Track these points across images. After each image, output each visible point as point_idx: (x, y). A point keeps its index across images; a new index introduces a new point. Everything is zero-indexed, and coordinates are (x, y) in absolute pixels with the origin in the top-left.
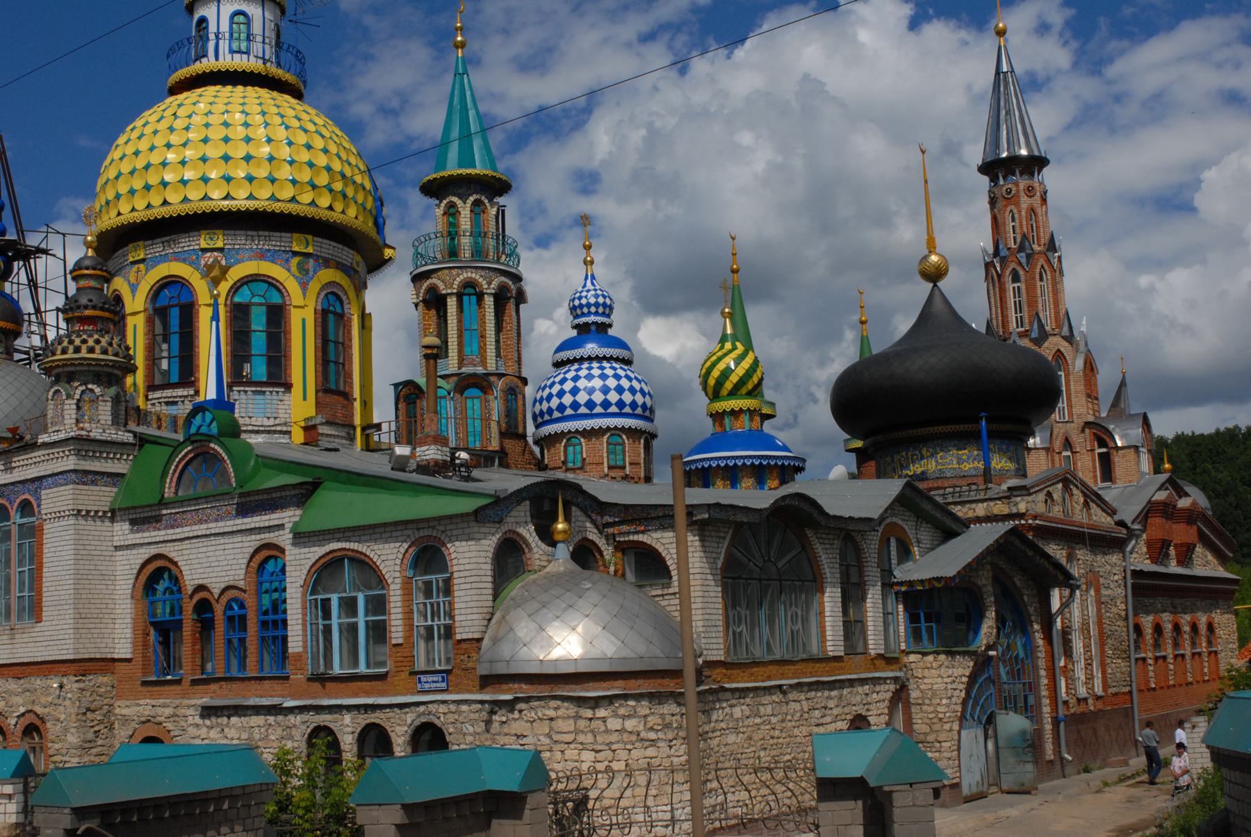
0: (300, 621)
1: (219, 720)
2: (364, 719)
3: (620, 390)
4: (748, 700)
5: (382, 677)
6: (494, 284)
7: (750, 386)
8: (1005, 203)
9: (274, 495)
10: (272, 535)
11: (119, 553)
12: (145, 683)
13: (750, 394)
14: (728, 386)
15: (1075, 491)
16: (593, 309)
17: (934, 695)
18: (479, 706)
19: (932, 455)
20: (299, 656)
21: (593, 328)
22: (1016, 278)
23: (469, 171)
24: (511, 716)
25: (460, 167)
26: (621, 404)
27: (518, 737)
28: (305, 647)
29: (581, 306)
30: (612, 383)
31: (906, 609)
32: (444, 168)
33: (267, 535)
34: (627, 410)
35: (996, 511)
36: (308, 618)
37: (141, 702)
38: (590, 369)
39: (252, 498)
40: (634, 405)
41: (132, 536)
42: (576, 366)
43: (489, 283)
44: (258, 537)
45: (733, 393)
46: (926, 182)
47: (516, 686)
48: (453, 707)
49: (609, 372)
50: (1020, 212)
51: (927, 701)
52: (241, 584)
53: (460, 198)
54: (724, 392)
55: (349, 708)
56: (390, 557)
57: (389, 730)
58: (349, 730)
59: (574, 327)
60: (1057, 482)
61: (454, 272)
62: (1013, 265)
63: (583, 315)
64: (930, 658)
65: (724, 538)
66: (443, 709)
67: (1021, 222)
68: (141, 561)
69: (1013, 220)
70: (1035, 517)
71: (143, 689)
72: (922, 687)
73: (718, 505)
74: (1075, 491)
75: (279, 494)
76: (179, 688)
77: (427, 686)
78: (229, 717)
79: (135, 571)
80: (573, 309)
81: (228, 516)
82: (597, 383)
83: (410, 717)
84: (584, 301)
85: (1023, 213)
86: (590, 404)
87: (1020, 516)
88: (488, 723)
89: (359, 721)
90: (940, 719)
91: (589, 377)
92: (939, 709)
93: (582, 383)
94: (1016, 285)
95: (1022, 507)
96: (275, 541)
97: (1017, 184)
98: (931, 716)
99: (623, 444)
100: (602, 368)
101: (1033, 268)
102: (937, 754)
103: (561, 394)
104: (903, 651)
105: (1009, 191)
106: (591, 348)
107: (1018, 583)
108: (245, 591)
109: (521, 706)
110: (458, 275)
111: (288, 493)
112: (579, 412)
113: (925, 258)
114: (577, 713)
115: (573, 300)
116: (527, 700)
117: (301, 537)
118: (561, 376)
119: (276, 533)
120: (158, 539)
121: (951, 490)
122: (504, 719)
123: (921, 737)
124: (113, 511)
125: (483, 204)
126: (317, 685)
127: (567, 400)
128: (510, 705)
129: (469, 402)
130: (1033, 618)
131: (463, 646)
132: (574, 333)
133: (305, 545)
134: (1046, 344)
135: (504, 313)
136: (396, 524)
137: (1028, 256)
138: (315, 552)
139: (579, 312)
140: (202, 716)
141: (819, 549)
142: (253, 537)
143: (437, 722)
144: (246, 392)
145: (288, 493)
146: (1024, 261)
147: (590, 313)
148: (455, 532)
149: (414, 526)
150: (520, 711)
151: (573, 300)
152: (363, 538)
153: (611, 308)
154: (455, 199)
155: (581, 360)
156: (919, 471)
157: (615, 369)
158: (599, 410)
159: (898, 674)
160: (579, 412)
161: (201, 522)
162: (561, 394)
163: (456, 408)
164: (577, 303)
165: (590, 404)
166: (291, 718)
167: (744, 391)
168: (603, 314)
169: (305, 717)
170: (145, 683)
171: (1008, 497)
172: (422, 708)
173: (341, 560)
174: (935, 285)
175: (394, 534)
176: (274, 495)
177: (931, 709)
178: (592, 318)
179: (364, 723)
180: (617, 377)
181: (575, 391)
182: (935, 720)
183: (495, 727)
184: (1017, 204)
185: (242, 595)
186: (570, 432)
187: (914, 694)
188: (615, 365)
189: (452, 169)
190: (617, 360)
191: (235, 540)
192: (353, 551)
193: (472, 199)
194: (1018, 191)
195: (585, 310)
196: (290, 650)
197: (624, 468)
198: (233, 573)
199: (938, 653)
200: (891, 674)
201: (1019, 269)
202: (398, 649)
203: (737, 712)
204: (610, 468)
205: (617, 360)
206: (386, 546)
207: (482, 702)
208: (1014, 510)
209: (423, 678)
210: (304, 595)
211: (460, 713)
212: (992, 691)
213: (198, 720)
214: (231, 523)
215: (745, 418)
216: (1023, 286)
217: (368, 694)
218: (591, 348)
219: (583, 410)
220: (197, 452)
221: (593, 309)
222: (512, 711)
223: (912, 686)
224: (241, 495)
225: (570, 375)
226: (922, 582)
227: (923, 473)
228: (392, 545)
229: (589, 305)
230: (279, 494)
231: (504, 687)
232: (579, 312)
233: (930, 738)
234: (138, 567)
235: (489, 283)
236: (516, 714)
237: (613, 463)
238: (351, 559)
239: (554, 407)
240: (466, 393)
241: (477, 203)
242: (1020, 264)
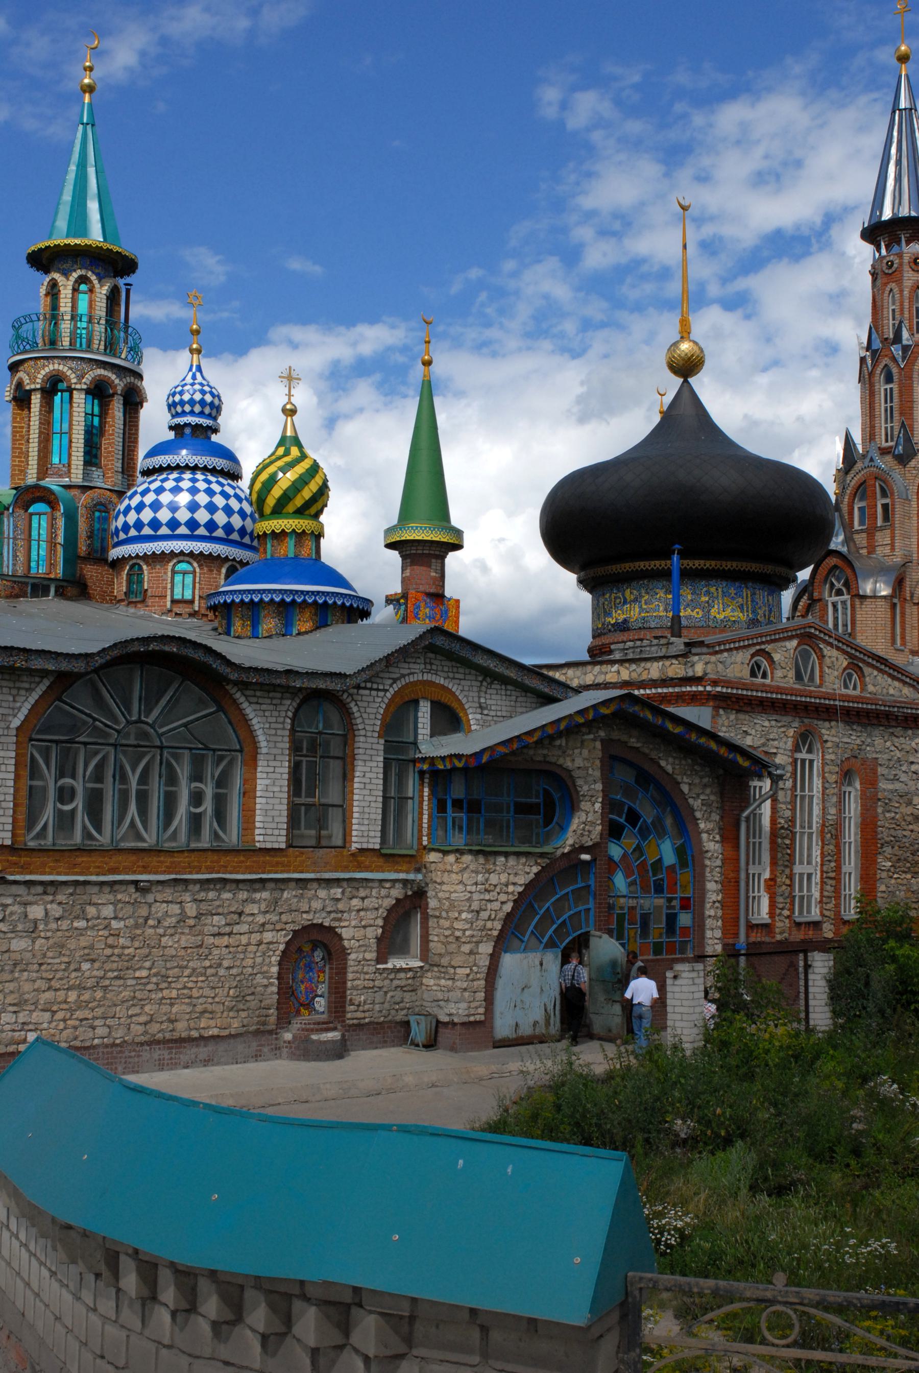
3: (228, 510)
4: (61, 898)
6: (88, 378)
7: (298, 502)
13: (300, 512)
14: (271, 502)
15: (828, 651)
16: (197, 409)
17: (452, 906)
19: (635, 600)
21: (188, 431)
22: (889, 379)
23: (78, 241)
25: (67, 237)
26: (211, 525)
29: (182, 403)
30: (202, 499)
31: (432, 793)
32: (50, 238)
34: (202, 531)
35: (671, 674)
38: (178, 480)
40: (228, 528)
42: (175, 475)
43: (81, 377)
45: (278, 510)
46: (685, 247)
49: (202, 485)
50: (901, 291)
51: (444, 914)
53: (97, 275)
54: (268, 510)
59: (171, 428)
60: (790, 638)
61: (40, 363)
62: (885, 361)
63: (184, 413)
64: (451, 858)
65: (30, 690)
67: (902, 304)
70: (715, 683)
72: (440, 895)
73: (104, 650)
74: (828, 651)
80: (171, 406)
82: (184, 498)
84: (186, 397)
85: (906, 293)
86: (173, 524)
87: (697, 680)
90: (457, 938)
91: (176, 490)
92: (456, 925)
93: (165, 498)
94: (888, 387)
95: (699, 670)
98: (447, 933)
99: (194, 572)
100: (194, 480)
102: (450, 983)
103: (140, 507)
104: (425, 847)
106: (184, 456)
107: (669, 769)
112: (160, 532)
113: (675, 344)
115: (174, 395)
118: (145, 486)
121: (630, 644)
123: (436, 959)
125: (91, 282)
127: (147, 515)
129: (35, 519)
130: (698, 815)
132: (171, 435)
134: (913, 463)
135: (107, 414)
139: (179, 409)
141: (249, 711)
151: (174, 395)
153: (218, 409)
154: (56, 276)
155: (170, 468)
156: (621, 618)
157: (222, 485)
158: (164, 531)
159: (411, 876)
160: (160, 532)
162: (140, 507)
163: (15, 526)
164: (177, 398)
165: (173, 524)
167: (291, 508)
168: (210, 416)
171: (684, 656)
174: (686, 381)
177: (446, 924)
180: (210, 492)
181: (156, 506)
182: (451, 939)
184: (899, 282)
186: (137, 556)
187: (433, 903)
188: (210, 478)
189: (60, 239)
190: (214, 471)
193: (75, 275)
194: (901, 264)
197: (192, 602)
199: (460, 852)
200: (402, 876)
201: (892, 365)
203: (36, 912)
204: (174, 602)
205: (214, 471)
208: (690, 674)
212: (591, 905)
215: (291, 542)
216: (894, 386)
218: (184, 456)
219: (147, 531)
221: (187, 408)
223: (430, 894)
225: (154, 486)
226: (443, 758)
227: (625, 621)
232: (179, 409)
233: (445, 961)
235: (81, 377)
237: (178, 596)
239: (131, 523)
240: (31, 510)
241: (83, 279)
242: (894, 359)
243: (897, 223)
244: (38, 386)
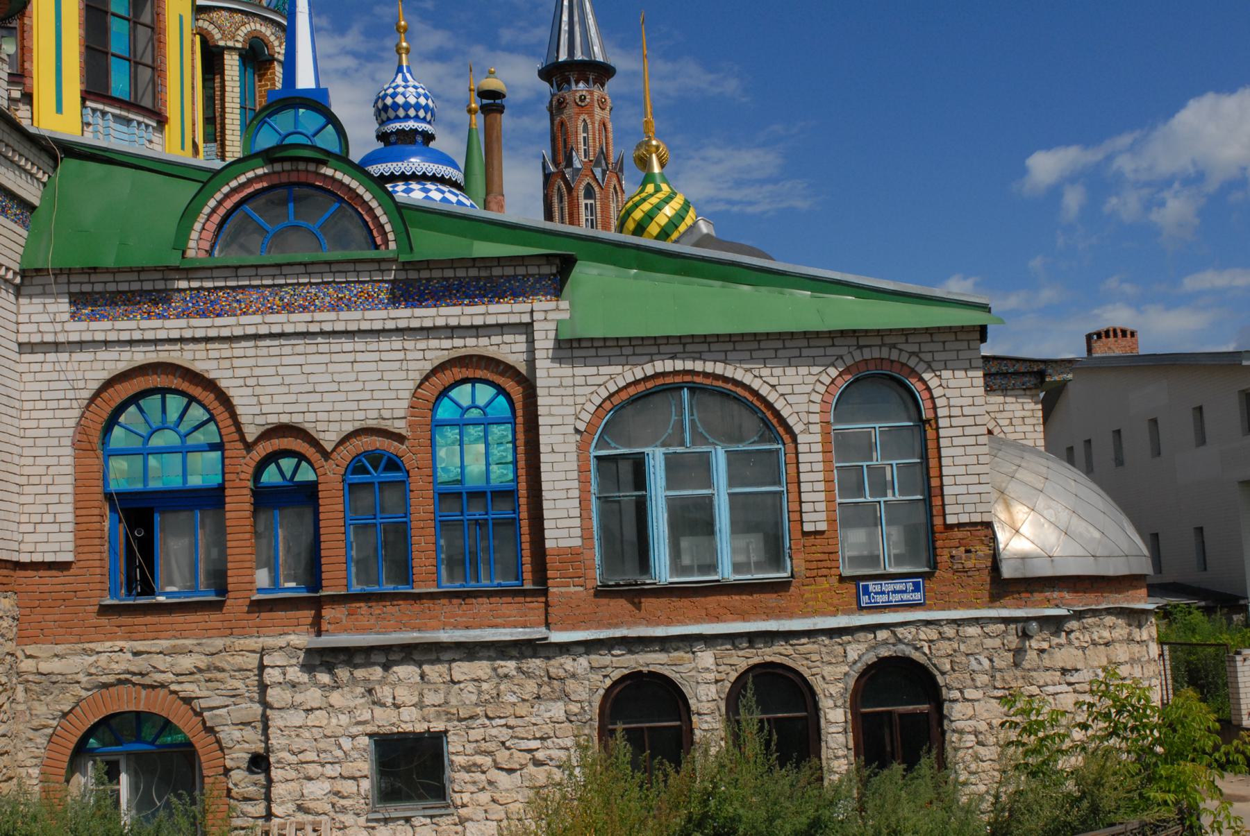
0: (576, 493)
1: (360, 673)
2: (743, 659)
5: (779, 587)
8: (577, 110)
9: (497, 272)
10: (484, 341)
11: (27, 358)
12: (105, 610)
18: (1002, 627)
20: (572, 556)
22: (589, 193)
24: (1055, 641)
27: (1064, 671)
28: (586, 536)
29: (396, 106)
33: (471, 342)
36: (594, 488)
37: (98, 647)
39: (437, 274)
41: (71, 326)
44: (447, 344)
47: (1056, 595)
48: (949, 631)
50: (593, 123)
52: (400, 426)
55: (709, 640)
56: (800, 393)
57: (806, 673)
58: (711, 676)
61: (238, 17)
63: (397, 118)
66: (932, 633)
68: (106, 375)
69: (586, 130)
71: (104, 621)
75: (509, 271)
76: (213, 618)
77: (881, 599)
78: (386, 667)
79: (87, 394)
81: (370, 301)
83: (858, 652)
88: (1019, 652)
89: (734, 660)
94: (589, 202)
96: (491, 352)
97: (591, 93)
101: (608, 184)
105: (582, 99)
108: (400, 438)
109: (1073, 624)
110: (244, 24)
111: (533, 270)
114: (1130, 634)
116: (1079, 615)
117: (571, 348)
119: (496, 339)
120: (162, 335)
122: (1045, 645)
124: (24, 273)
126: (622, 605)
128: (1055, 625)
131: (958, 534)
133: (572, 361)
136: (809, 337)
137: (604, 173)
138: (620, 375)
140: (308, 668)
142: (434, 343)
143: (916, 656)
144: (104, 113)
145: (533, 270)
146: (599, 177)
147: (407, 117)
148: (938, 356)
149: (853, 341)
150: (1068, 633)
152: (730, 356)
161: (288, 308)
166: (567, 662)
169: (598, 659)
170: (105, 610)
172: (882, 635)
173: (679, 388)
175: (805, 352)
176: (497, 272)
178: (411, 124)
179: (743, 665)
183: (1031, 657)
184: (591, 115)
185: (392, 447)
191: (384, 345)
192: (706, 375)
194: (592, 100)
195: (401, 113)
196: (549, 544)
198: (379, 404)
201: (594, 184)
202: (811, 540)
206: (791, 371)
207: (1006, 621)
209: (873, 586)
210: (582, 448)
211: (963, 639)
213: (295, 674)
214: (382, 314)
217: (743, 616)
220: (276, 181)
222: (1057, 633)
224: (406, 266)
228: (803, 370)
229: (407, 106)
230: (509, 271)
231: (1038, 596)
232: (391, 114)
234: (95, 386)
236: (1063, 640)
238: (693, 389)
243: (571, 65)
244: (239, 45)
